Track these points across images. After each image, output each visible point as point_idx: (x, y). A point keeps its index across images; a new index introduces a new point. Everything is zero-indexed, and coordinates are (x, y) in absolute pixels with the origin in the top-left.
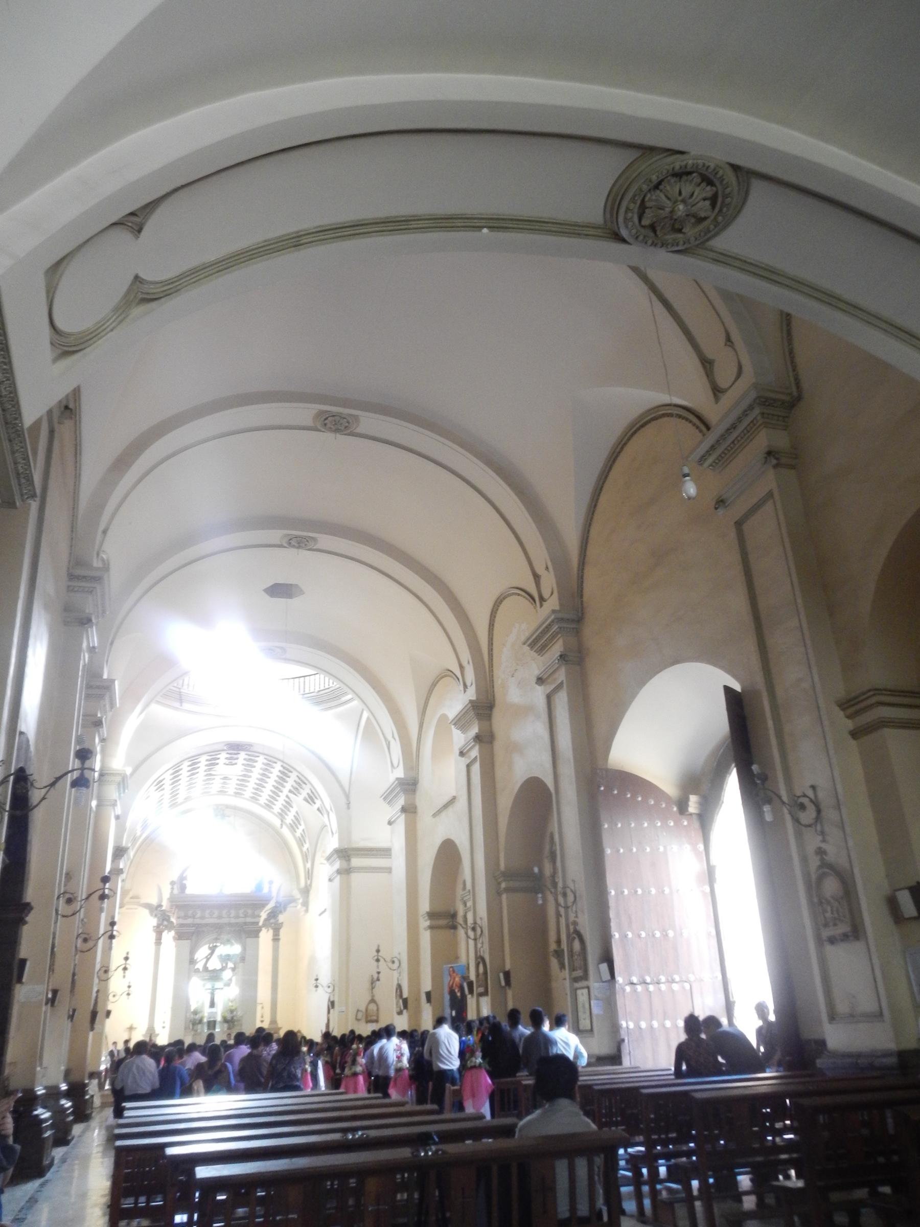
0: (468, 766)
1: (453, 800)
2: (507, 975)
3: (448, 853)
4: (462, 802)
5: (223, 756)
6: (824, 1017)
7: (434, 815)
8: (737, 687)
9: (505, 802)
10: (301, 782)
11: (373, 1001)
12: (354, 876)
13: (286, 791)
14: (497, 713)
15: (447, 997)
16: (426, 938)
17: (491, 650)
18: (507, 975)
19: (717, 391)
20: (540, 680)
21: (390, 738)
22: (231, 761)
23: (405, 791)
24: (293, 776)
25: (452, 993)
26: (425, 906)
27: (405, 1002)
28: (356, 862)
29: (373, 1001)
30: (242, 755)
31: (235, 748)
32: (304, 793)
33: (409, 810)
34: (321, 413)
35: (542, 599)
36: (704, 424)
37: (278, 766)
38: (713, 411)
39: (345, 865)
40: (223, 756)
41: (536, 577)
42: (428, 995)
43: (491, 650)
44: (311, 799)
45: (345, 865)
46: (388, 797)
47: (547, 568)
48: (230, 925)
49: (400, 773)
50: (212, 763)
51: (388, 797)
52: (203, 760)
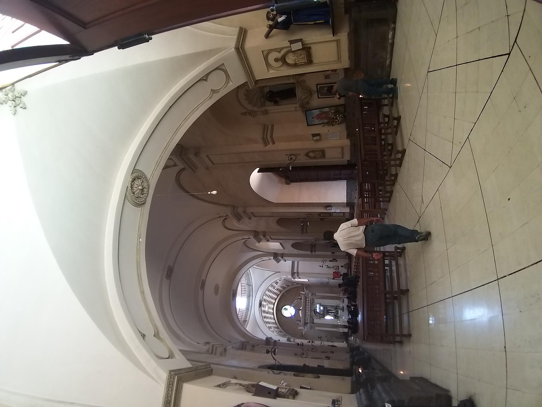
3: (294, 246)
4: (282, 241)
5: (263, 309)
6: (343, 159)
8: (258, 169)
9: (282, 229)
11: (333, 267)
12: (299, 271)
14: (258, 230)
15: (333, 248)
16: (317, 253)
17: (239, 231)
19: (175, 165)
20: (250, 218)
22: (264, 306)
24: (270, 288)
25: (332, 247)
26: (309, 253)
27: (334, 259)
28: (295, 271)
29: (333, 267)
30: (263, 303)
31: (260, 305)
33: (283, 255)
34: (166, 277)
35: (227, 216)
36: (183, 170)
38: (181, 166)
39: (296, 274)
40: (263, 309)
41: (220, 217)
43: (239, 231)
45: (296, 274)
46: (278, 261)
50: (265, 312)
51: (278, 261)
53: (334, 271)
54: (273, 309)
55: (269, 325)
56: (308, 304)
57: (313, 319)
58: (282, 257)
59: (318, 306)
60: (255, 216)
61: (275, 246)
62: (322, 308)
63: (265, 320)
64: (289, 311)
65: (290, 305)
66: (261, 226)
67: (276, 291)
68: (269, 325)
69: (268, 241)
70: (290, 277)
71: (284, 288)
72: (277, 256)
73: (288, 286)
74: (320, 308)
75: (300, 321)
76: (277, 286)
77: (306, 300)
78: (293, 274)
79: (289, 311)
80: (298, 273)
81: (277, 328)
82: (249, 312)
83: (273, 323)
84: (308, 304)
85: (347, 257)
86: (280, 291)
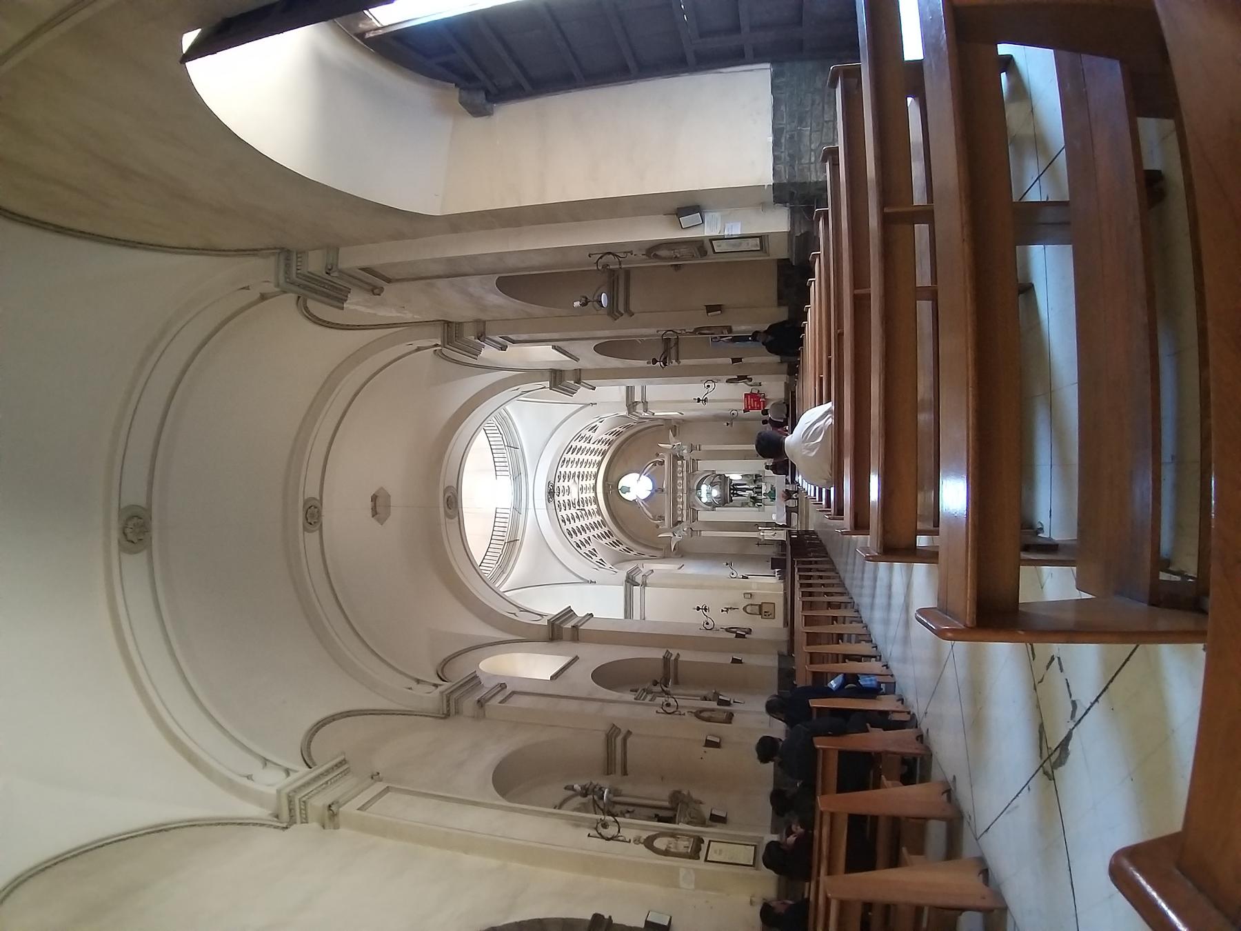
0: (513, 342)
1: (554, 347)
2: (710, 309)
5: (561, 498)
7: (577, 360)
9: (537, 310)
10: (579, 437)
13: (588, 446)
18: (710, 309)
20: (375, 291)
21: (519, 392)
23: (561, 381)
24: (574, 444)
28: (637, 398)
30: (560, 484)
31: (551, 493)
32: (589, 434)
33: (579, 377)
37: (568, 456)
42: (734, 361)
44: (594, 429)
47: (247, 288)
48: (688, 481)
49: (547, 384)
52: (563, 513)
53: (748, 390)
54: (595, 488)
55: (582, 537)
56: (682, 475)
57: (695, 512)
58: (578, 381)
59: (704, 488)
60: (389, 281)
61: (544, 355)
62: (715, 493)
63: (569, 526)
64: (637, 486)
65: (640, 472)
66: (456, 303)
67: (596, 446)
68: (582, 537)
69: (504, 348)
70: (625, 413)
71: (618, 434)
72: (558, 379)
73: (628, 427)
74: (709, 493)
75: (662, 518)
76: (595, 436)
77: (675, 466)
78: (631, 406)
79: (637, 486)
80: (645, 403)
81: (609, 534)
82: (522, 517)
83: (595, 526)
84: (682, 475)
85: (785, 367)
86: (610, 443)
